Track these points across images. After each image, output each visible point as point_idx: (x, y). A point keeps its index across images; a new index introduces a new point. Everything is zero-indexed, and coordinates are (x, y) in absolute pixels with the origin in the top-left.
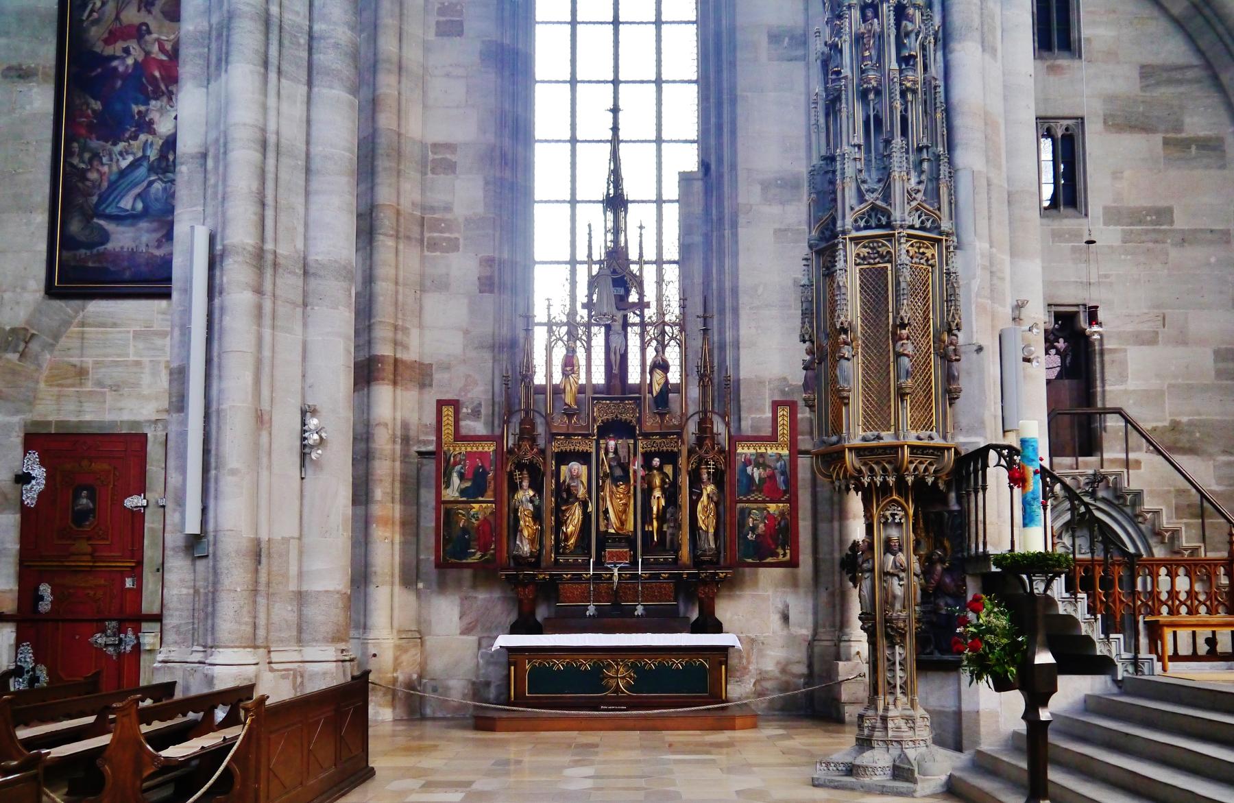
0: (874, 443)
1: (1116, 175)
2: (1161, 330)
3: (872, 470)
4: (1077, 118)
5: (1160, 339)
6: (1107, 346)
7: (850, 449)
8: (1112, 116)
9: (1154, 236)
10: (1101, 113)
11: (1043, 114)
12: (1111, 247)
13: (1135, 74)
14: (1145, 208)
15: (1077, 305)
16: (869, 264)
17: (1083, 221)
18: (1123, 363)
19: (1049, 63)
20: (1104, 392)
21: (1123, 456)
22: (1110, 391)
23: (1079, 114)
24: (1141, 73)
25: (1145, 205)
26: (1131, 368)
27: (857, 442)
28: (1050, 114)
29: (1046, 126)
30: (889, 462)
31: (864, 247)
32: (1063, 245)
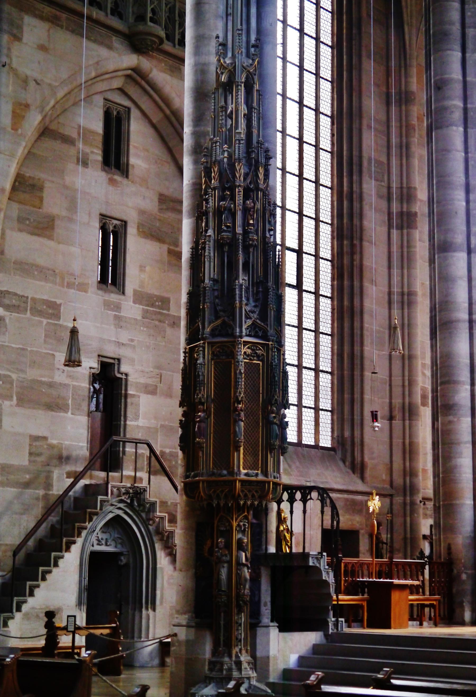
0: (254, 478)
1: (142, 268)
2: (158, 385)
3: (246, 495)
4: (122, 221)
5: (158, 391)
6: (130, 392)
7: (240, 481)
8: (143, 225)
9: (159, 317)
10: (136, 221)
11: (104, 212)
12: (136, 319)
13: (156, 199)
14: (156, 296)
15: (114, 359)
16: (250, 359)
17: (122, 297)
18: (138, 405)
19: (110, 176)
20: (125, 425)
21: (133, 474)
22: (129, 425)
23: (124, 218)
24: (159, 199)
25: (156, 293)
26: (142, 409)
27: (243, 477)
28: (108, 214)
29: (104, 221)
30: (257, 492)
31: (248, 348)
32: (110, 312)
